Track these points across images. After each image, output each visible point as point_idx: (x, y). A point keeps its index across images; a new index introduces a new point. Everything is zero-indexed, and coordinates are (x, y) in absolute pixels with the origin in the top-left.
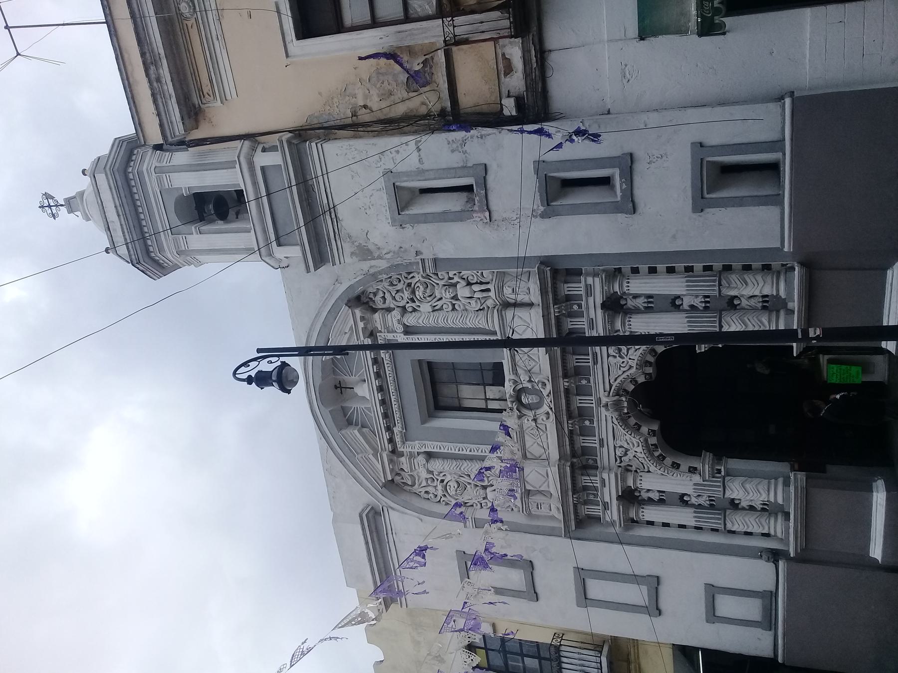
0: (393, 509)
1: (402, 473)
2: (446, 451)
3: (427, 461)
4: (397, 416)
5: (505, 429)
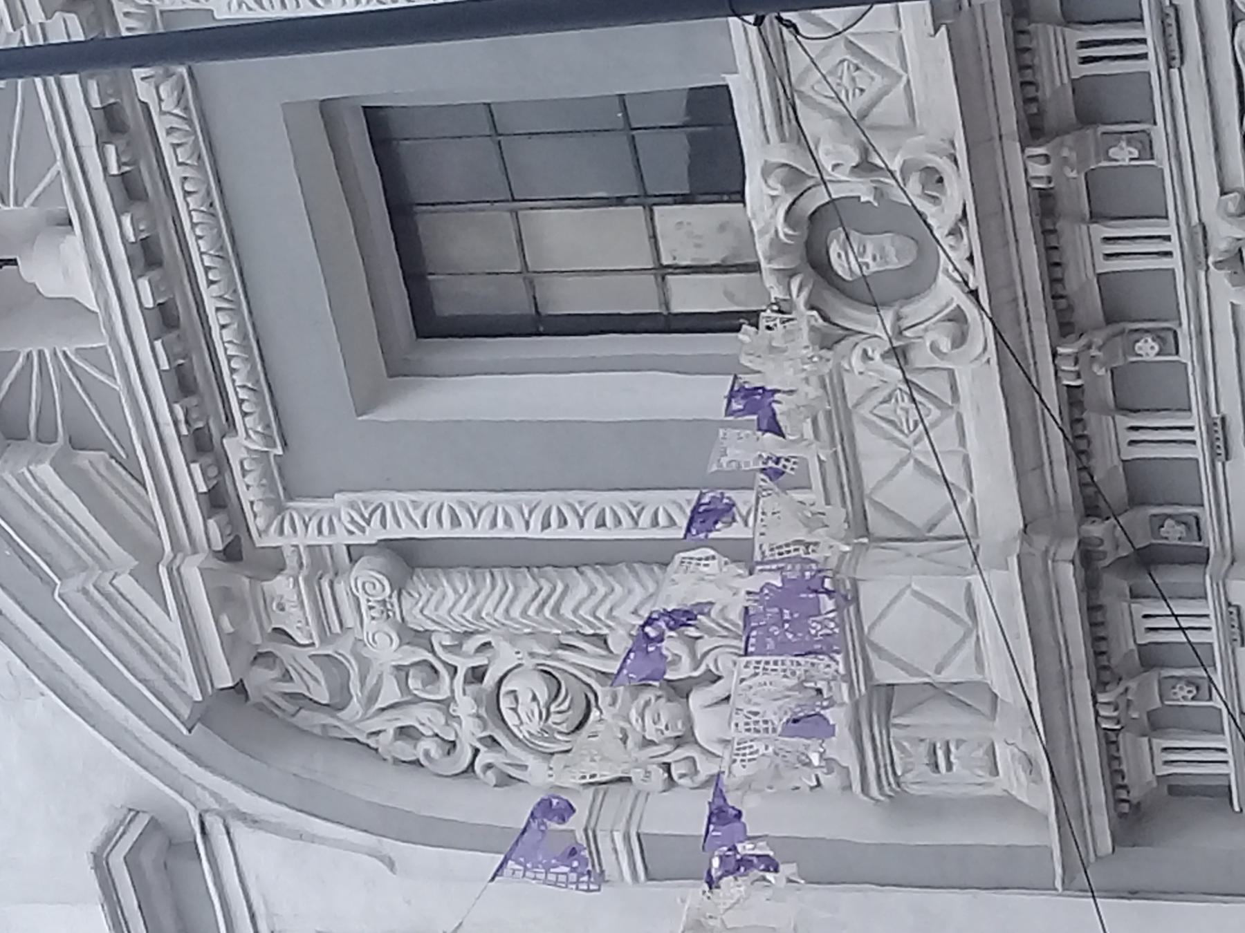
0: (253, 822)
1: (283, 651)
2: (483, 531)
3: (399, 589)
4: (237, 381)
5: (754, 402)
